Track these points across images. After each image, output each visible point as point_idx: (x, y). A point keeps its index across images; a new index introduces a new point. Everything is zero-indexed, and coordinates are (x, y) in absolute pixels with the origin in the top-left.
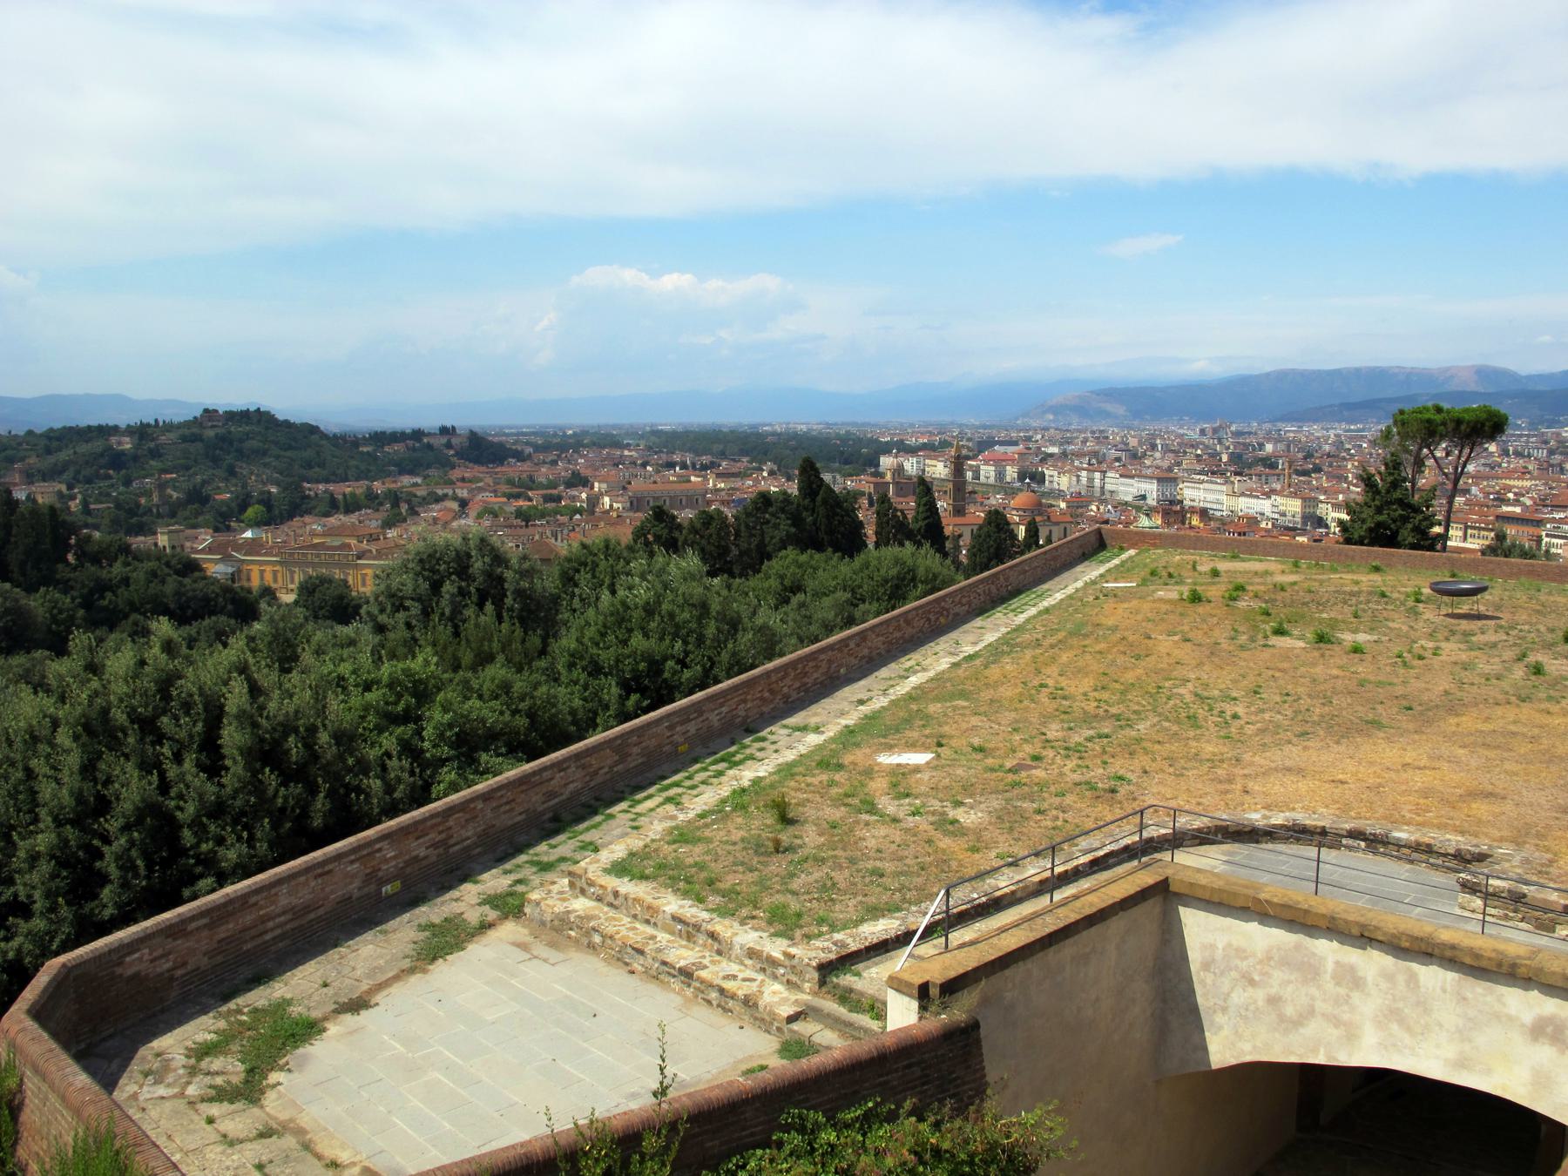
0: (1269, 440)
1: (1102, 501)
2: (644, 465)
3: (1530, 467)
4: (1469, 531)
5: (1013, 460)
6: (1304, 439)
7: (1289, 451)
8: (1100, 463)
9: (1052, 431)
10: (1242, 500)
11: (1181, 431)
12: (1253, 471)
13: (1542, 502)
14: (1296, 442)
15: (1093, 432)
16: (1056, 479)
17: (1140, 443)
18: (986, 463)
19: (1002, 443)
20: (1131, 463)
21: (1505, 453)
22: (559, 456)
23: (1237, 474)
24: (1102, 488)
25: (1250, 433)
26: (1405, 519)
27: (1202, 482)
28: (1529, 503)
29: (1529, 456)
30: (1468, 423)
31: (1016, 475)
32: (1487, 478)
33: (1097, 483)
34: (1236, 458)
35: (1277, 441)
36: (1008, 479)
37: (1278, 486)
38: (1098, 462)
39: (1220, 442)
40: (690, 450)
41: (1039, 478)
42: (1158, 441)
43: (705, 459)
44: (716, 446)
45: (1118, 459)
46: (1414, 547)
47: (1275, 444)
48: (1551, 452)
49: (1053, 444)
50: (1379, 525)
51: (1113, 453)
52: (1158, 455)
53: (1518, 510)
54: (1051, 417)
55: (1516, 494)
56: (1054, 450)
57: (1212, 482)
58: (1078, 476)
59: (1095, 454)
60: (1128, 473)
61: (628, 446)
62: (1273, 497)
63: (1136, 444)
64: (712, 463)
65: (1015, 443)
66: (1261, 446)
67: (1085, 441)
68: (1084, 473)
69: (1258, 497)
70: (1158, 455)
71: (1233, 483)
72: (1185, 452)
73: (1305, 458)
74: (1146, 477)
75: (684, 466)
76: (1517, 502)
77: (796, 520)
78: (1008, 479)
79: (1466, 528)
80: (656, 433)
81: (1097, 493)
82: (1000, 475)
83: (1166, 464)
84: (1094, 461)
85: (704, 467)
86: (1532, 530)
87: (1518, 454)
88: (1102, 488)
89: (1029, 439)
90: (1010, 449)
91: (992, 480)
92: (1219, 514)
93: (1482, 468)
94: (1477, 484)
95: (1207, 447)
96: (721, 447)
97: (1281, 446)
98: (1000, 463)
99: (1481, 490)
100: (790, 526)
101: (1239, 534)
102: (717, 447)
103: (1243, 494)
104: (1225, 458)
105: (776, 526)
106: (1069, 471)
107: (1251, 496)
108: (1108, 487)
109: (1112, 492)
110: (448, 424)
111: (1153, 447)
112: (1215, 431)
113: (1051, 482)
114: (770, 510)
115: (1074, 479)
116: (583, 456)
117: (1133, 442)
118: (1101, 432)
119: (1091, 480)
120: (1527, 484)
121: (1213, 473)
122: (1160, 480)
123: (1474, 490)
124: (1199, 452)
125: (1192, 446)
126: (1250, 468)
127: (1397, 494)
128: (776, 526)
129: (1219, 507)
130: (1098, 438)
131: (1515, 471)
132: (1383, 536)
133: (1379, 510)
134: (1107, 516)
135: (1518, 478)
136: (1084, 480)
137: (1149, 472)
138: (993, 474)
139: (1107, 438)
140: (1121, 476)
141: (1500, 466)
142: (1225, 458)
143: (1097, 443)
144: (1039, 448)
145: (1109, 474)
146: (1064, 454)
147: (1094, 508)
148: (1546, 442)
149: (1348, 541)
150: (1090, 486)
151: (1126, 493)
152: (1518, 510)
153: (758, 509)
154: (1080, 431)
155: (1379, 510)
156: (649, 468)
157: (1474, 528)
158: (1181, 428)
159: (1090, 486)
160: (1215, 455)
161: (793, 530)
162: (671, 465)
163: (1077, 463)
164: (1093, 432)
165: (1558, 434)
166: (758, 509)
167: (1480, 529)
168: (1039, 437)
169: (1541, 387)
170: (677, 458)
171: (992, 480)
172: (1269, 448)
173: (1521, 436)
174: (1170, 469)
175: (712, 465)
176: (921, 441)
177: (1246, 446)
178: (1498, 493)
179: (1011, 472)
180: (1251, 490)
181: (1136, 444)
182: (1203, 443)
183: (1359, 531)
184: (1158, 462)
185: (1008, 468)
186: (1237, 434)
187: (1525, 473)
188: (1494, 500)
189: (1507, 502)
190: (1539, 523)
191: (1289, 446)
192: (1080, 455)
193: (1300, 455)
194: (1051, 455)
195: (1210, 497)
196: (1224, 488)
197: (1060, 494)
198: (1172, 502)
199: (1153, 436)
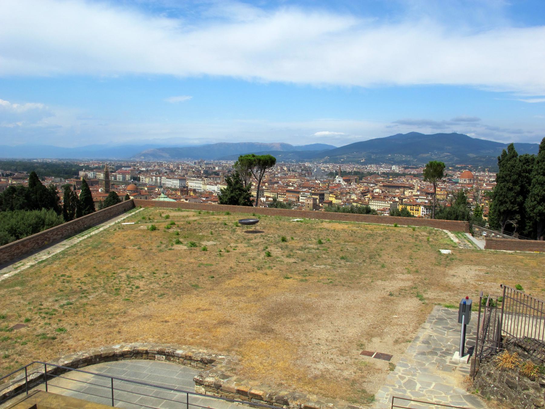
0: (217, 166)
1: (161, 187)
3: (296, 175)
4: (279, 195)
5: (129, 173)
6: (228, 166)
7: (223, 169)
8: (159, 174)
10: (208, 186)
11: (188, 163)
12: (211, 176)
13: (299, 186)
14: (225, 167)
15: (158, 163)
16: (144, 179)
17: (174, 167)
18: (119, 174)
19: (125, 167)
20: (171, 174)
21: (289, 170)
23: (206, 177)
24: (160, 182)
25: (211, 164)
26: (240, 195)
27: (194, 180)
28: (296, 186)
29: (296, 171)
30: (263, 161)
31: (130, 178)
32: (284, 178)
33: (159, 181)
34: (206, 172)
35: (219, 166)
36: (127, 179)
37: (219, 181)
38: (159, 173)
39: (201, 166)
41: (139, 179)
42: (180, 166)
43: (8, 172)
45: (166, 172)
46: (245, 204)
47: (219, 168)
48: (302, 170)
49: (143, 167)
50: (232, 197)
51: (164, 170)
52: (180, 171)
53: (293, 188)
54: (143, 158)
55: (292, 183)
56: (144, 169)
57: (197, 180)
58: (152, 178)
59: (158, 171)
60: (169, 177)
62: (218, 185)
65: (130, 167)
66: (214, 168)
67: (155, 166)
68: (154, 177)
69: (213, 185)
70: (180, 171)
71: (204, 180)
72: (189, 170)
73: (228, 172)
76: (292, 186)
77: (27, 197)
78: (127, 179)
79: (278, 194)
81: (159, 183)
82: (124, 178)
83: (182, 174)
84: (157, 173)
85: (7, 175)
86: (296, 195)
87: (293, 171)
88: (160, 182)
89: (135, 165)
90: (128, 169)
91: (121, 180)
92: (200, 191)
93: (282, 175)
94: (280, 180)
95: (196, 168)
96: (15, 168)
97: (221, 168)
98: (124, 174)
99: (282, 182)
100: (24, 199)
101: (206, 198)
102: (13, 168)
103: (208, 184)
104: (202, 172)
105: (18, 200)
106: (149, 177)
107: (210, 185)
108: (163, 182)
109: (164, 184)
111: (178, 168)
112: (199, 163)
113: (142, 180)
114: (15, 193)
115: (151, 179)
117: (171, 166)
118: (160, 163)
119: (156, 180)
120: (295, 180)
121: (198, 177)
122: (180, 180)
123: (280, 182)
124: (194, 170)
125: (192, 168)
126: (210, 175)
127: (238, 186)
128: (18, 200)
129: (200, 189)
130: (159, 165)
131: (292, 176)
132: (233, 201)
133: (232, 192)
135: (293, 178)
136: (154, 180)
137: (176, 177)
138: (121, 178)
139: (163, 165)
140: (167, 178)
141: (288, 174)
142: (202, 172)
143: (159, 167)
144: (138, 169)
145: (163, 178)
146: (147, 171)
147: (157, 190)
148: (301, 167)
149: (222, 203)
151: (169, 184)
152: (293, 188)
153: (10, 193)
154: (153, 163)
155: (232, 192)
157: (280, 194)
158: (188, 161)
160: (199, 171)
161: (26, 201)
163: (151, 174)
164: (158, 163)
165: (304, 165)
166: (10, 193)
167: (282, 194)
169: (299, 150)
171: (121, 180)
172: (217, 168)
173: (294, 165)
174: (184, 176)
175: (11, 175)
176: (95, 166)
177: (209, 168)
178: (287, 183)
179: (128, 177)
180: (211, 183)
182: (195, 167)
183: (226, 200)
184: (180, 173)
185: (127, 176)
186: (207, 164)
187: (295, 177)
188: (286, 185)
189: (290, 186)
190: (299, 192)
191: (223, 168)
192: (152, 171)
193: (227, 171)
194: (143, 171)
195: (197, 185)
196: (202, 182)
197: (145, 185)
198: (184, 187)
199: (178, 164)
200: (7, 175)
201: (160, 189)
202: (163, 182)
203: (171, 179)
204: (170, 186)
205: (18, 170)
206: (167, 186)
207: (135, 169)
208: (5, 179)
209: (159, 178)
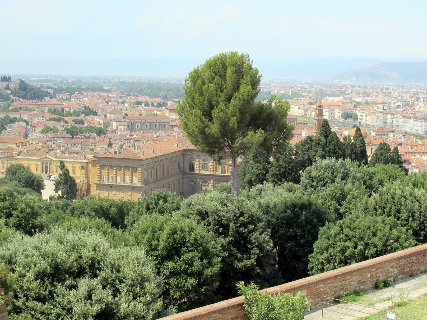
2: (123, 103)
5: (339, 106)
8: (389, 109)
9: (357, 88)
15: (382, 89)
17: (411, 97)
19: (330, 95)
22: (71, 96)
31: (340, 115)
33: (389, 120)
40: (149, 95)
43: (157, 100)
44: (162, 92)
45: (399, 107)
49: (358, 95)
54: (355, 79)
58: (378, 116)
59: (386, 103)
61: (109, 91)
63: (408, 97)
64: (164, 103)
65: (338, 96)
67: (377, 95)
68: (381, 115)
70: (422, 104)
74: (418, 118)
75: (147, 105)
78: (336, 118)
80: (122, 83)
85: (160, 106)
89: (343, 92)
90: (336, 99)
96: (165, 93)
102: (164, 93)
108: (395, 123)
109: (397, 126)
110: (7, 76)
111: (418, 99)
115: (376, 118)
116: (85, 97)
117: (406, 96)
118: (387, 89)
119: (385, 118)
130: (385, 93)
134: (400, 141)
136: (381, 119)
137: (419, 115)
140: (403, 117)
144: (351, 99)
145: (395, 116)
147: (392, 136)
150: (385, 123)
154: (373, 88)
156: (126, 105)
159: (385, 123)
162: (139, 103)
163: (375, 108)
164: (382, 89)
168: (350, 91)
170: (141, 99)
175: (164, 104)
176: (280, 92)
181: (408, 97)
194: (359, 103)
200: (160, 106)
201: (396, 136)
202: (395, 123)
203: (410, 118)
204: (408, 130)
205: (169, 96)
206: (403, 129)
207: (346, 99)
208: (158, 111)
209: (389, 116)
